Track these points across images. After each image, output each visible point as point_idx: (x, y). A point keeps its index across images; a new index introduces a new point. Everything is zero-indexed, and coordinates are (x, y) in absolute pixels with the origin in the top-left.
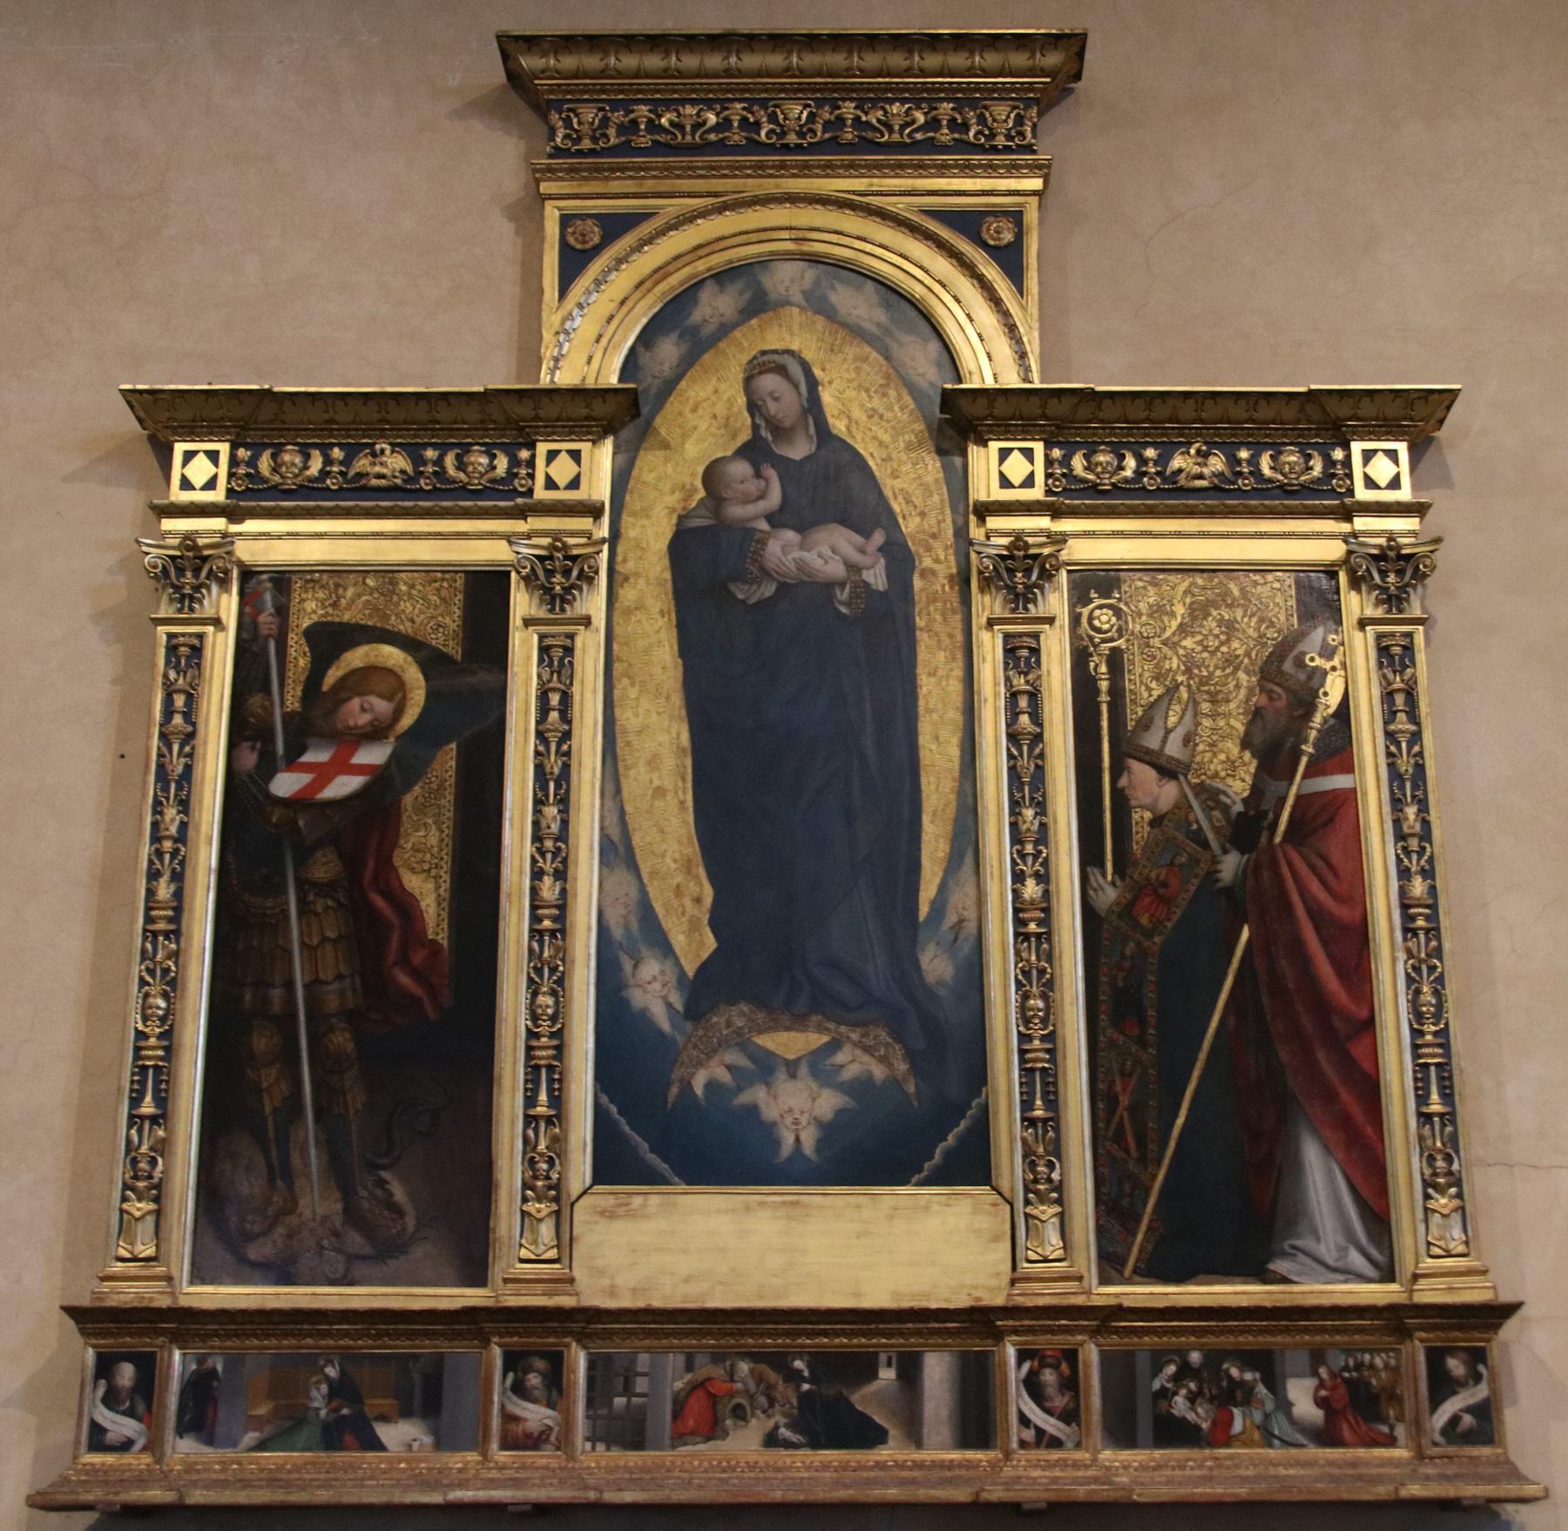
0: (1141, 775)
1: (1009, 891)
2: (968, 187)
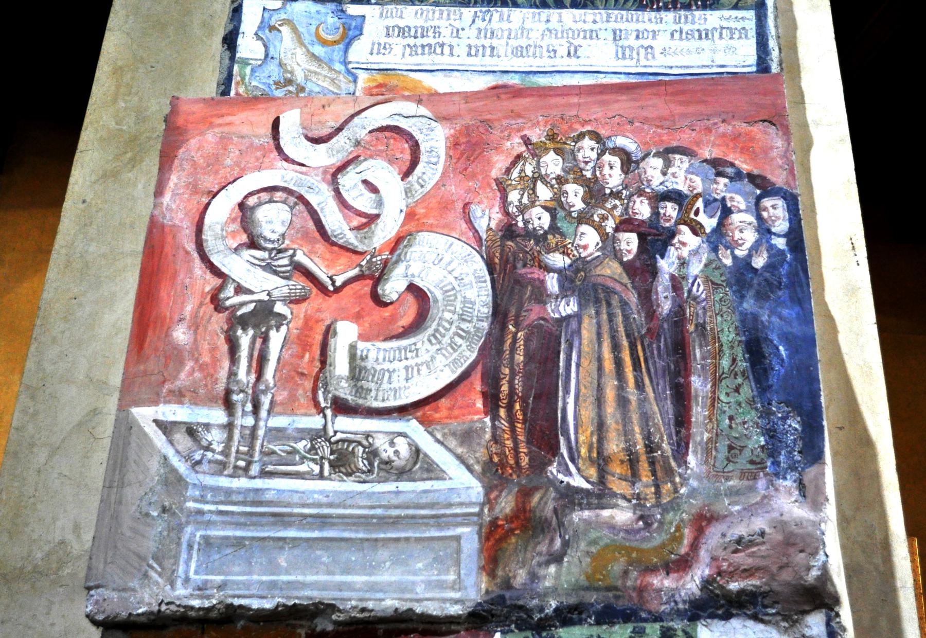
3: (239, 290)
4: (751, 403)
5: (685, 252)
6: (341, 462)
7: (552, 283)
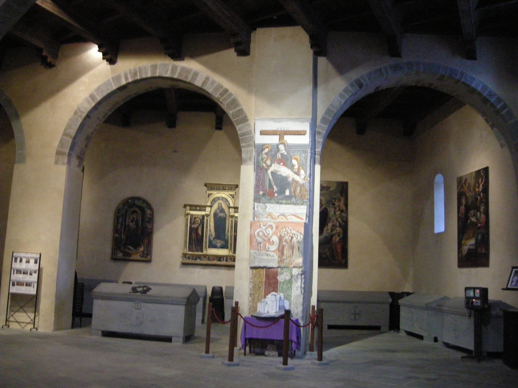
6: (267, 255)
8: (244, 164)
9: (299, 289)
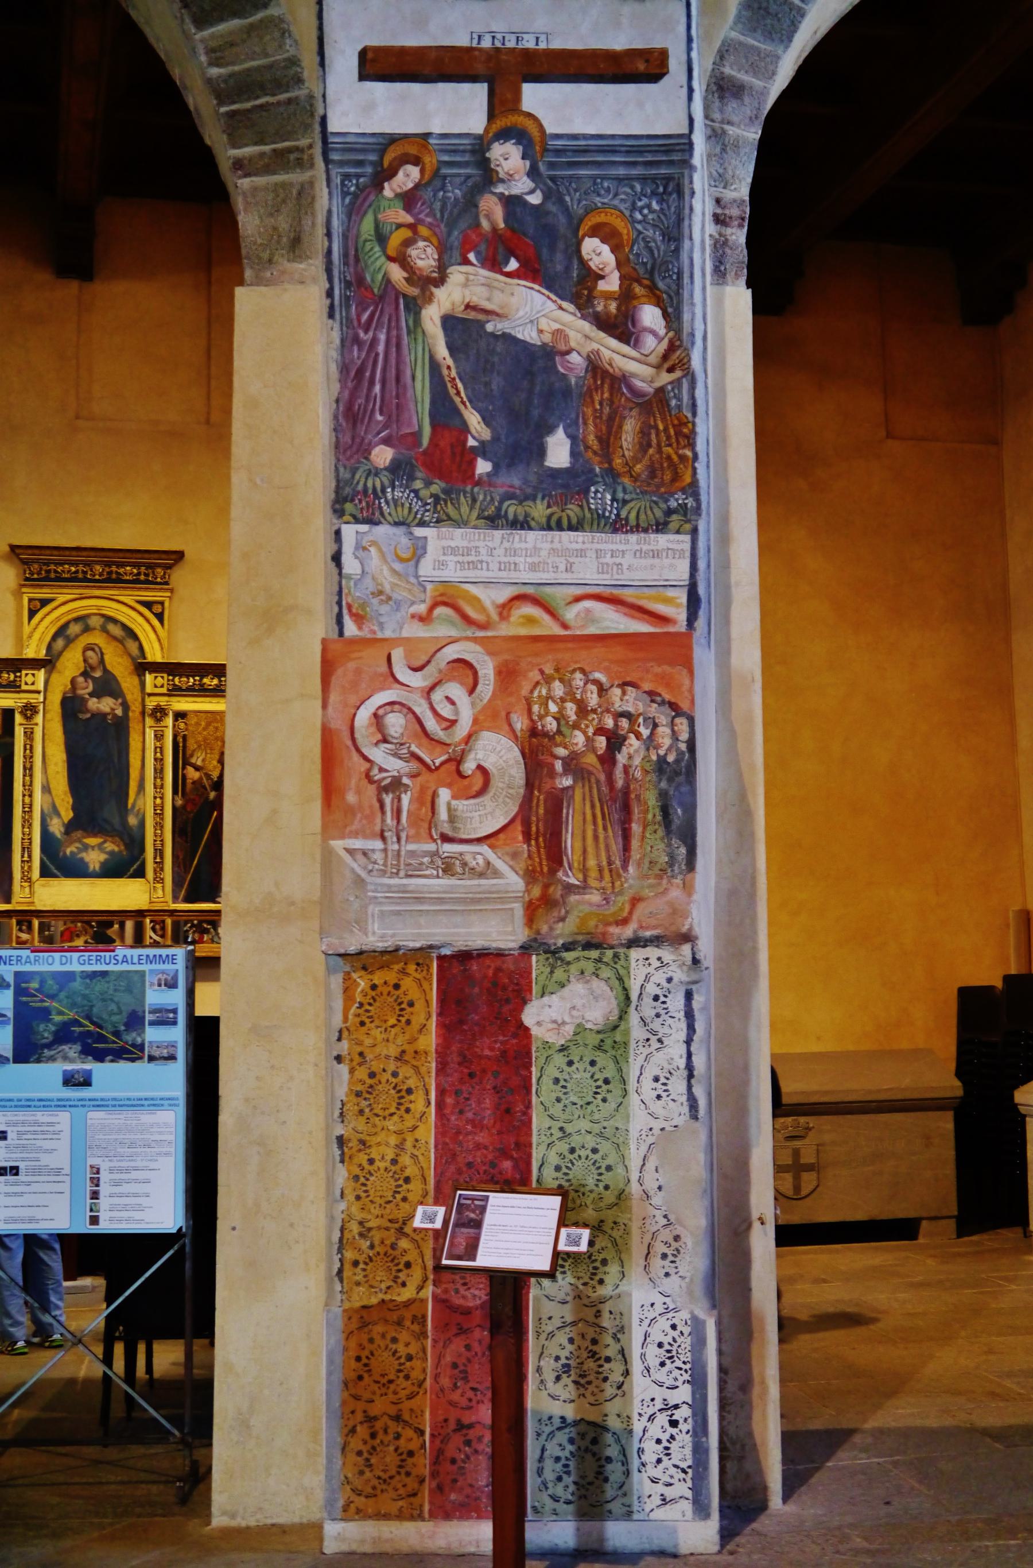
0: (190, 770)
1: (152, 802)
2: (149, 596)
3: (381, 770)
4: (662, 839)
5: (632, 750)
6: (448, 870)
7: (558, 766)
8: (259, 281)
9: (678, 1086)
